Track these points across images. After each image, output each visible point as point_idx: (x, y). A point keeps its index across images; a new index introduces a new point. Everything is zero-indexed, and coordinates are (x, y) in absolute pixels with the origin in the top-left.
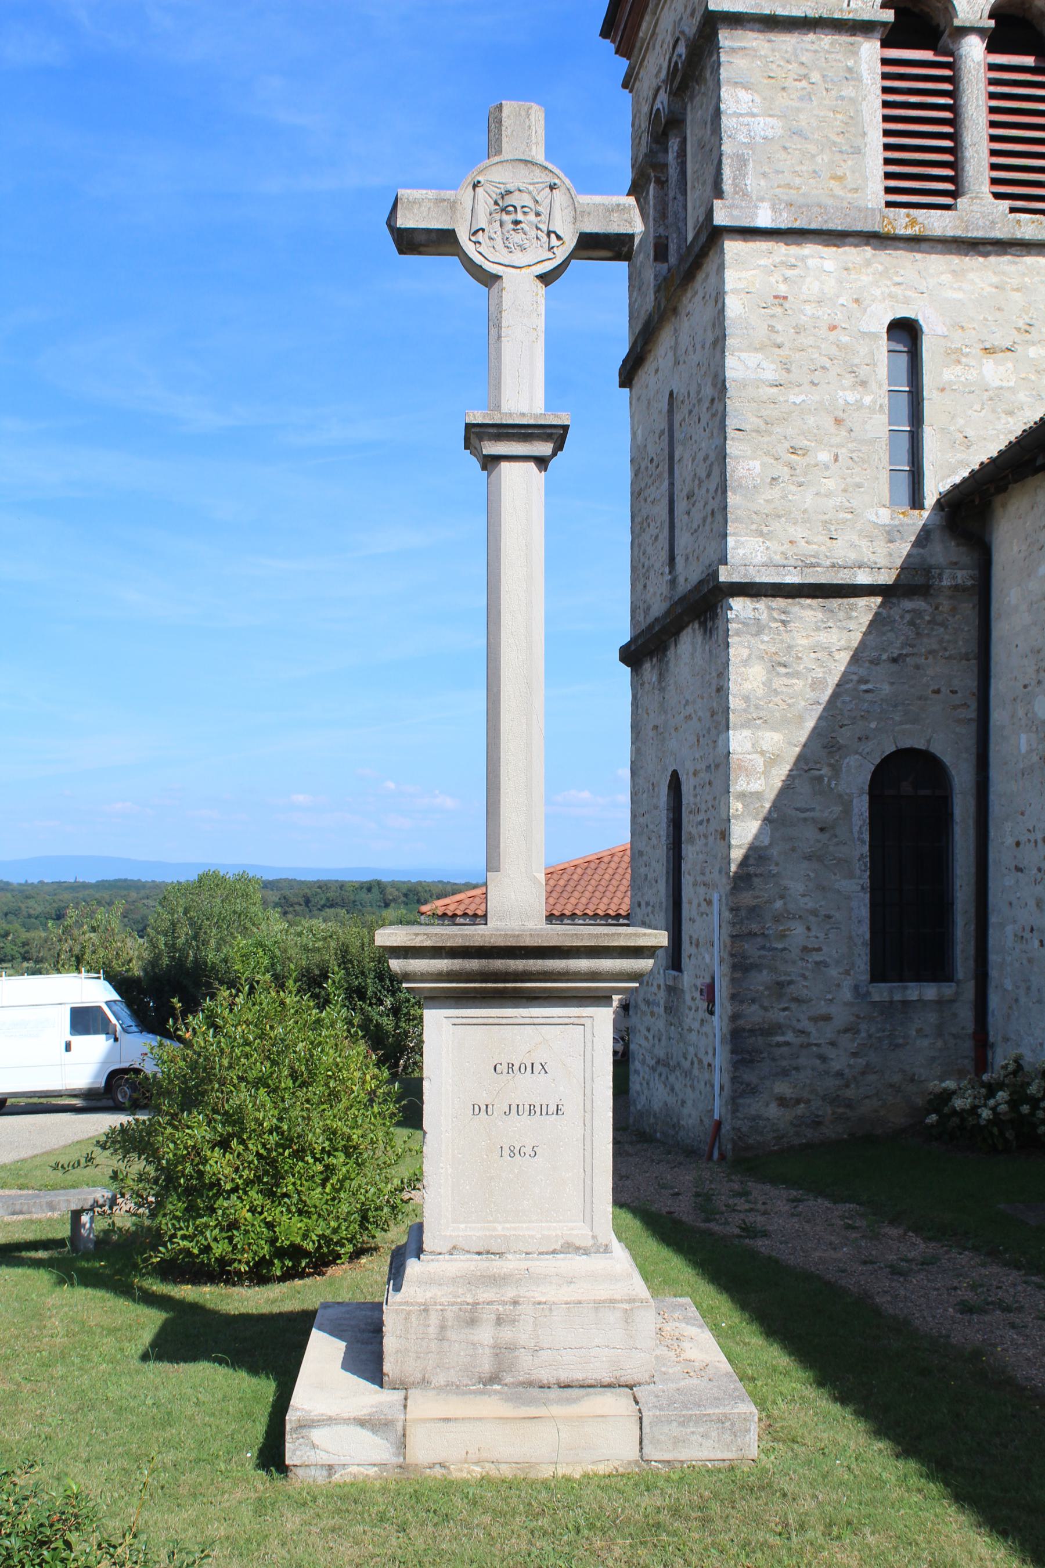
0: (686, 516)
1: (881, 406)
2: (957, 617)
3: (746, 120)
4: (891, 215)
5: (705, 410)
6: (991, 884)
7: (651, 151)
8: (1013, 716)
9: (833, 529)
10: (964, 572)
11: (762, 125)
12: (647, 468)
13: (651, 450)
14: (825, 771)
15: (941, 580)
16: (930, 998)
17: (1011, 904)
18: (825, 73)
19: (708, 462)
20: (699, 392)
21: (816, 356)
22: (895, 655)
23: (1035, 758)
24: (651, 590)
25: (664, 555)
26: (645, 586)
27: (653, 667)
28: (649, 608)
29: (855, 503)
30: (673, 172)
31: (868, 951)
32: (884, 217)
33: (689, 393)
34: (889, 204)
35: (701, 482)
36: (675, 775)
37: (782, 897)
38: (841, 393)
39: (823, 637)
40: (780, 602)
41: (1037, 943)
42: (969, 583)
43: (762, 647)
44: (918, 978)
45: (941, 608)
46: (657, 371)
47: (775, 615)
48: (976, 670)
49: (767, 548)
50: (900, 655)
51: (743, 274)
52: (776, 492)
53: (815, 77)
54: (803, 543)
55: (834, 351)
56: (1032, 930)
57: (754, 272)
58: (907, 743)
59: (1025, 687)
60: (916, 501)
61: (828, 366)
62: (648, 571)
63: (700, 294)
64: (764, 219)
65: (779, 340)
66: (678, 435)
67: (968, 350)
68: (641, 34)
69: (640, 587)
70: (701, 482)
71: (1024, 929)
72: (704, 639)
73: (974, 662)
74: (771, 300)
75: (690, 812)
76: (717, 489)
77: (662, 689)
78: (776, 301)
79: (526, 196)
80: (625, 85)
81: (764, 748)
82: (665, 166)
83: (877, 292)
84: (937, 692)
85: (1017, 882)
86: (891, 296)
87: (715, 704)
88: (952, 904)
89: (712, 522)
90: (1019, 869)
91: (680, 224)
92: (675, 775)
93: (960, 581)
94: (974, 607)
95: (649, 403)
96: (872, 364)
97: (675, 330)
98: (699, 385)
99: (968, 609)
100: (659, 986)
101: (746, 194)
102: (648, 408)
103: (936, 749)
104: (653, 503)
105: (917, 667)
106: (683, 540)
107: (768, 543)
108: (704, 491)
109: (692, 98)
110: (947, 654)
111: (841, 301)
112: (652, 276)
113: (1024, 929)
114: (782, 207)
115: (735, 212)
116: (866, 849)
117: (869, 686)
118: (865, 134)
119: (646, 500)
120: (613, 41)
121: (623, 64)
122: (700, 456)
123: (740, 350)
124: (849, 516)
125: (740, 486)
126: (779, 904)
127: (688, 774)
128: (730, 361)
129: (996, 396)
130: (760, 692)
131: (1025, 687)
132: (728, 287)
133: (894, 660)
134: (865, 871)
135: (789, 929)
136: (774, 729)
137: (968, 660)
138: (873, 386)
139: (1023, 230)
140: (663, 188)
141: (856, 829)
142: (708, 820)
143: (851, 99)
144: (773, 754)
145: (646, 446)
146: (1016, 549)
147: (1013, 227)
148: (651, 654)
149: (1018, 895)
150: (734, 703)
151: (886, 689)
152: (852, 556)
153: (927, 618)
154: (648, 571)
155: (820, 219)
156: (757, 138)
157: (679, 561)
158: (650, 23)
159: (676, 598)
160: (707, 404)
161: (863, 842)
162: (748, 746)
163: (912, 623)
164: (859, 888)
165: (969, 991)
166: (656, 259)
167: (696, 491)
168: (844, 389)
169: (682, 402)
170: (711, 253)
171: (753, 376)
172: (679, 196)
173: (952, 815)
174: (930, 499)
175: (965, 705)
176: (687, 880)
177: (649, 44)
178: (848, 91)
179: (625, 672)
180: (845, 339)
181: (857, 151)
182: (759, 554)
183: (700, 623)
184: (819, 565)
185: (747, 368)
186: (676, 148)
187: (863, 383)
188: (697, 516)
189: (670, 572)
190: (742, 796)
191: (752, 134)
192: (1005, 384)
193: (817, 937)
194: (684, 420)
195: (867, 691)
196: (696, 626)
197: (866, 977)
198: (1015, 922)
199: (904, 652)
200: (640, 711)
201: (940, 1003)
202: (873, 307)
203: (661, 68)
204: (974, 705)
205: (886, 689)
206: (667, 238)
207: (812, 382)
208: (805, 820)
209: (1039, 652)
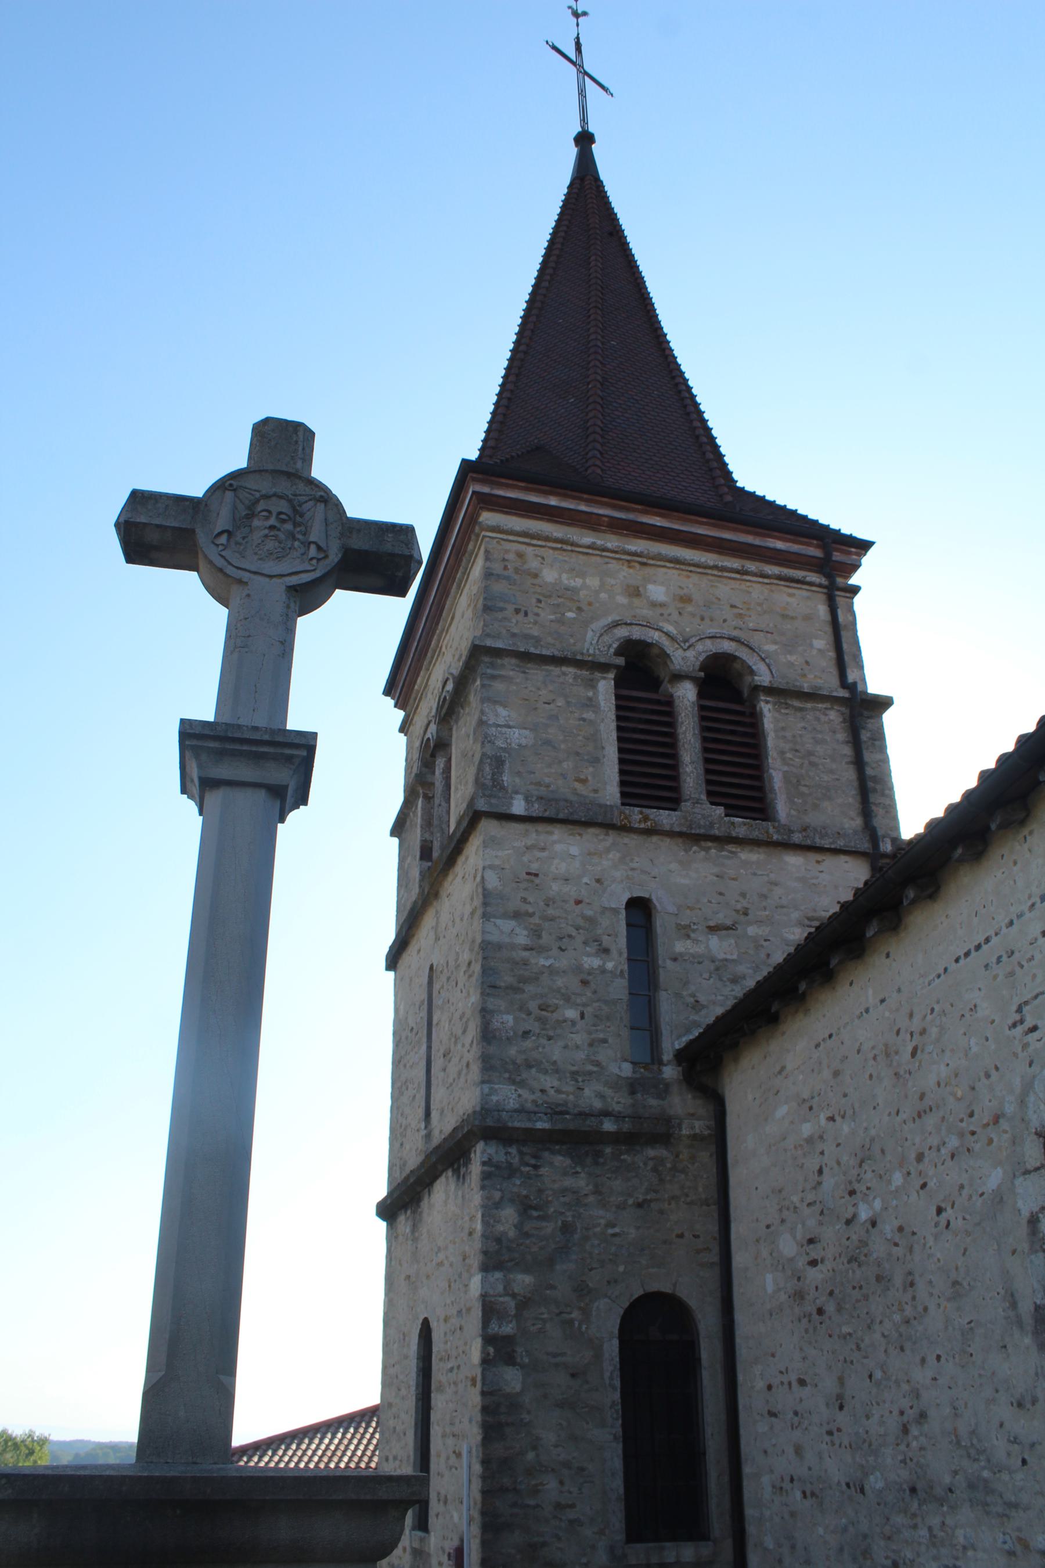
0: (442, 1074)
1: (622, 971)
2: (696, 1164)
3: (504, 730)
4: (627, 812)
5: (462, 973)
6: (742, 1431)
7: (421, 772)
8: (756, 1258)
9: (580, 1079)
10: (701, 1122)
11: (516, 735)
12: (407, 1038)
13: (411, 1022)
14: (575, 1315)
15: (680, 1130)
16: (688, 1560)
17: (765, 1452)
18: (570, 700)
19: (464, 1020)
20: (457, 960)
21: (563, 925)
22: (640, 1200)
23: (783, 1297)
24: (408, 1147)
25: (421, 1112)
26: (402, 1145)
27: (407, 1219)
28: (404, 1164)
29: (600, 1057)
30: (439, 785)
31: (623, 1508)
32: (621, 813)
33: (447, 962)
35: (457, 1039)
36: (426, 1323)
37: (534, 1448)
38: (585, 959)
41: (798, 1495)
42: (706, 1132)
43: (515, 1190)
44: (674, 1538)
45: (681, 1156)
46: (419, 951)
47: (527, 1158)
48: (716, 1215)
49: (520, 1096)
50: (645, 1200)
51: (500, 853)
52: (528, 1044)
54: (552, 1092)
55: (580, 922)
56: (792, 1480)
57: (509, 852)
58: (654, 1287)
59: (768, 1227)
61: (573, 934)
62: (405, 1129)
63: (460, 876)
65: (531, 910)
66: (437, 1001)
67: (695, 927)
68: (416, 687)
69: (398, 1145)
70: (457, 1039)
71: (782, 1479)
72: (457, 1185)
73: (714, 1207)
74: (524, 876)
75: (441, 1359)
76: (472, 1042)
77: (415, 1240)
78: (528, 877)
79: (283, 503)
80: (402, 729)
81: (516, 1291)
82: (433, 784)
84: (681, 1236)
85: (772, 1428)
86: (628, 877)
87: (467, 1248)
88: (704, 1454)
89: (467, 1074)
90: (772, 1414)
91: (444, 826)
92: (426, 1323)
93: (697, 1131)
94: (711, 1156)
95: (411, 980)
97: (437, 912)
98: (457, 954)
99: (706, 1157)
100: (405, 1549)
101: (503, 788)
102: (410, 985)
103: (683, 1293)
104: (411, 1067)
105: (661, 1212)
106: (439, 1094)
107: (520, 1091)
108: (459, 1046)
109: (457, 722)
110: (689, 1199)
111: (585, 880)
112: (418, 873)
113: (782, 1479)
114: (534, 800)
115: (493, 801)
116: (617, 1396)
117: (617, 1230)
118: (603, 748)
119: (405, 1066)
120: (393, 698)
121: (400, 714)
122: (457, 1015)
123: (495, 917)
124: (595, 1069)
125: (494, 1037)
126: (531, 1456)
127: (438, 1321)
129: (720, 967)
130: (512, 1234)
131: (768, 1227)
133: (639, 1205)
134: (617, 1419)
135: (542, 1484)
136: (527, 1271)
137: (708, 1205)
138: (614, 953)
139: (737, 830)
140: (429, 802)
141: (607, 1375)
142: (459, 1367)
143: (591, 721)
144: (525, 1297)
145: (407, 1018)
146: (750, 1097)
147: (729, 827)
148: (404, 1207)
149: (774, 1441)
151: (633, 1233)
152: (598, 1104)
153: (669, 1165)
154: (405, 1129)
155: (566, 811)
156: (513, 745)
157: (435, 1115)
158: (424, 677)
159: (431, 1149)
160: (464, 968)
161: (614, 1388)
162: (500, 1288)
163: (655, 1170)
164: (612, 1437)
165: (727, 1547)
166: (422, 858)
167: (452, 1049)
168: (589, 955)
169: (441, 972)
170: (470, 839)
171: (507, 940)
172: (443, 804)
173: (699, 1359)
175: (708, 1249)
176: (435, 1431)
177: (422, 694)
178: (589, 715)
179: (383, 1225)
181: (596, 761)
182: (511, 1101)
183: (454, 1171)
184: (567, 1113)
185: (502, 932)
186: (442, 766)
187: (606, 951)
188: (453, 1069)
189: (426, 1127)
191: (509, 741)
192: (729, 957)
193: (570, 1493)
194: (442, 987)
195: (614, 1235)
196: (450, 1173)
197: (621, 1537)
198: (772, 1472)
199: (648, 1197)
200: (393, 1263)
202: (613, 886)
203: (431, 709)
204: (716, 1249)
205: (633, 1233)
206: (432, 842)
207: (560, 948)
208: (557, 1365)
209: (780, 1191)
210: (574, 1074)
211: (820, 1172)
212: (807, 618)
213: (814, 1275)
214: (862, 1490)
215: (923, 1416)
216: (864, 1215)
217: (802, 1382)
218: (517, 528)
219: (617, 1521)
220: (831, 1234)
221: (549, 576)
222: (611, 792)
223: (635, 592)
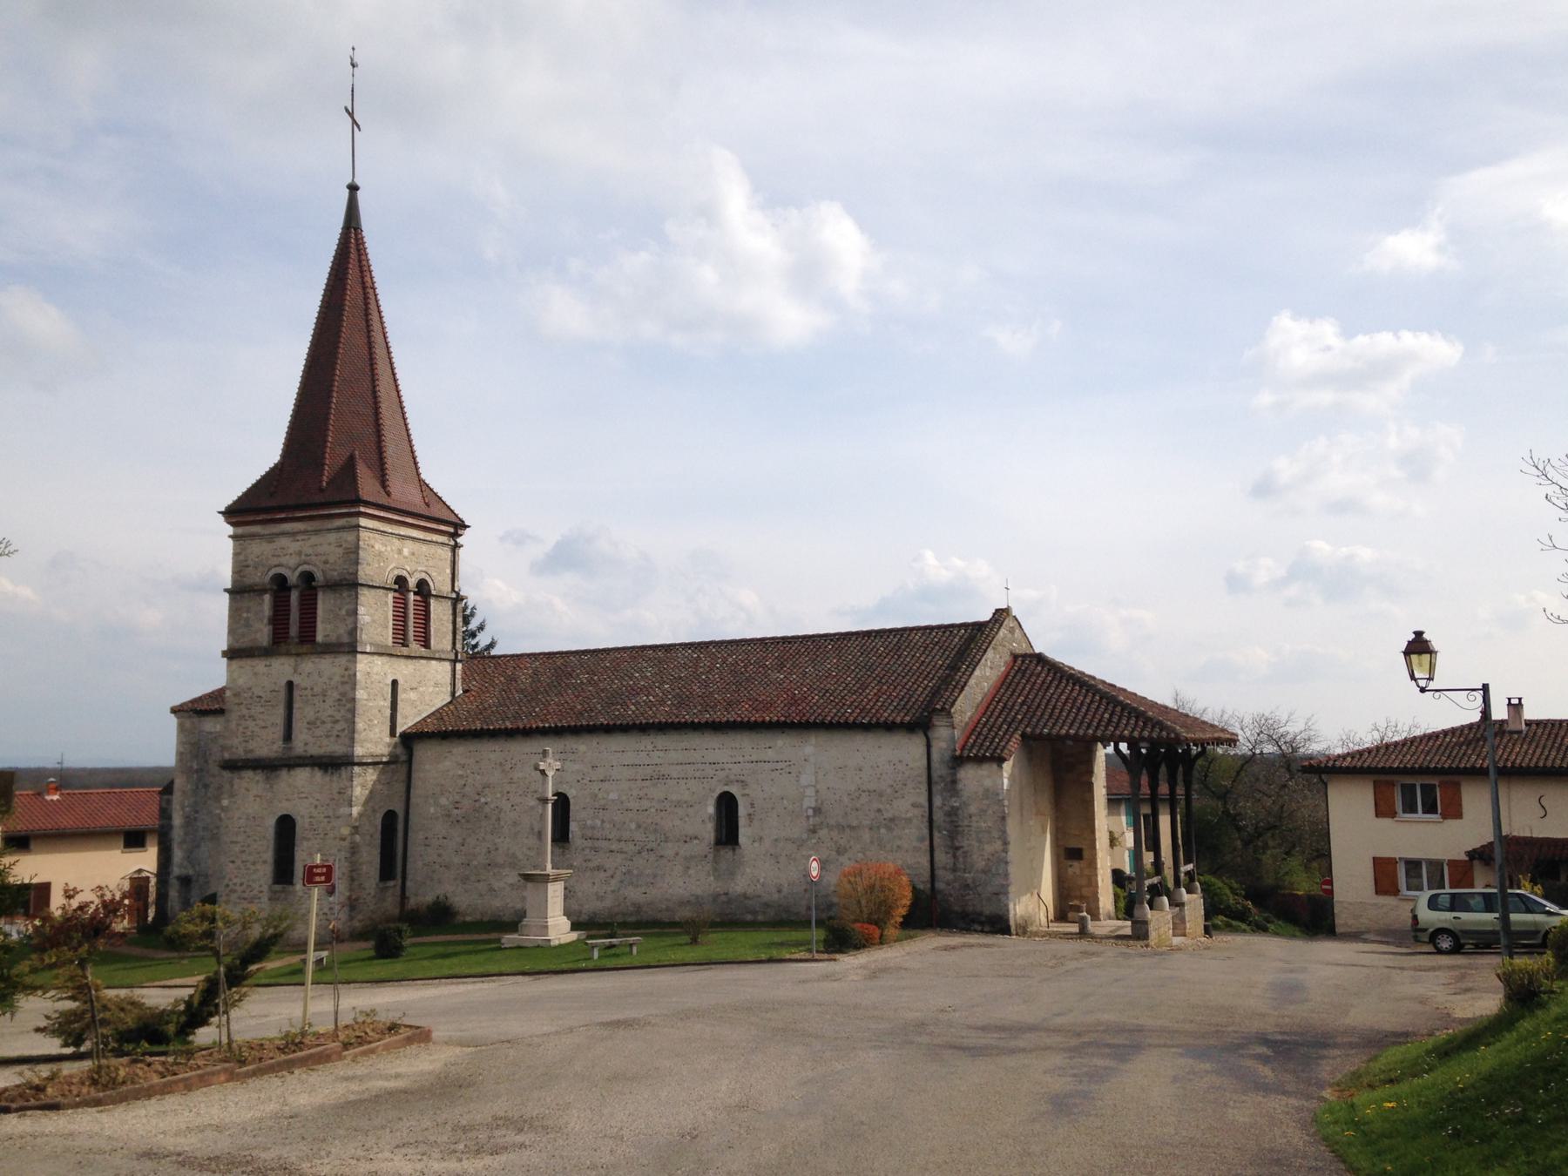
34: (394, 643)
40: (365, 767)
60: (393, 733)
64: (368, 651)
103: (397, 810)
151: (386, 792)
174: (398, 735)
181: (387, 627)
201: (395, 886)
205: (386, 792)
213: (456, 811)
215: (497, 849)
216: (483, 800)
217: (444, 838)
218: (371, 526)
220: (466, 803)
222: (390, 641)
223: (400, 552)
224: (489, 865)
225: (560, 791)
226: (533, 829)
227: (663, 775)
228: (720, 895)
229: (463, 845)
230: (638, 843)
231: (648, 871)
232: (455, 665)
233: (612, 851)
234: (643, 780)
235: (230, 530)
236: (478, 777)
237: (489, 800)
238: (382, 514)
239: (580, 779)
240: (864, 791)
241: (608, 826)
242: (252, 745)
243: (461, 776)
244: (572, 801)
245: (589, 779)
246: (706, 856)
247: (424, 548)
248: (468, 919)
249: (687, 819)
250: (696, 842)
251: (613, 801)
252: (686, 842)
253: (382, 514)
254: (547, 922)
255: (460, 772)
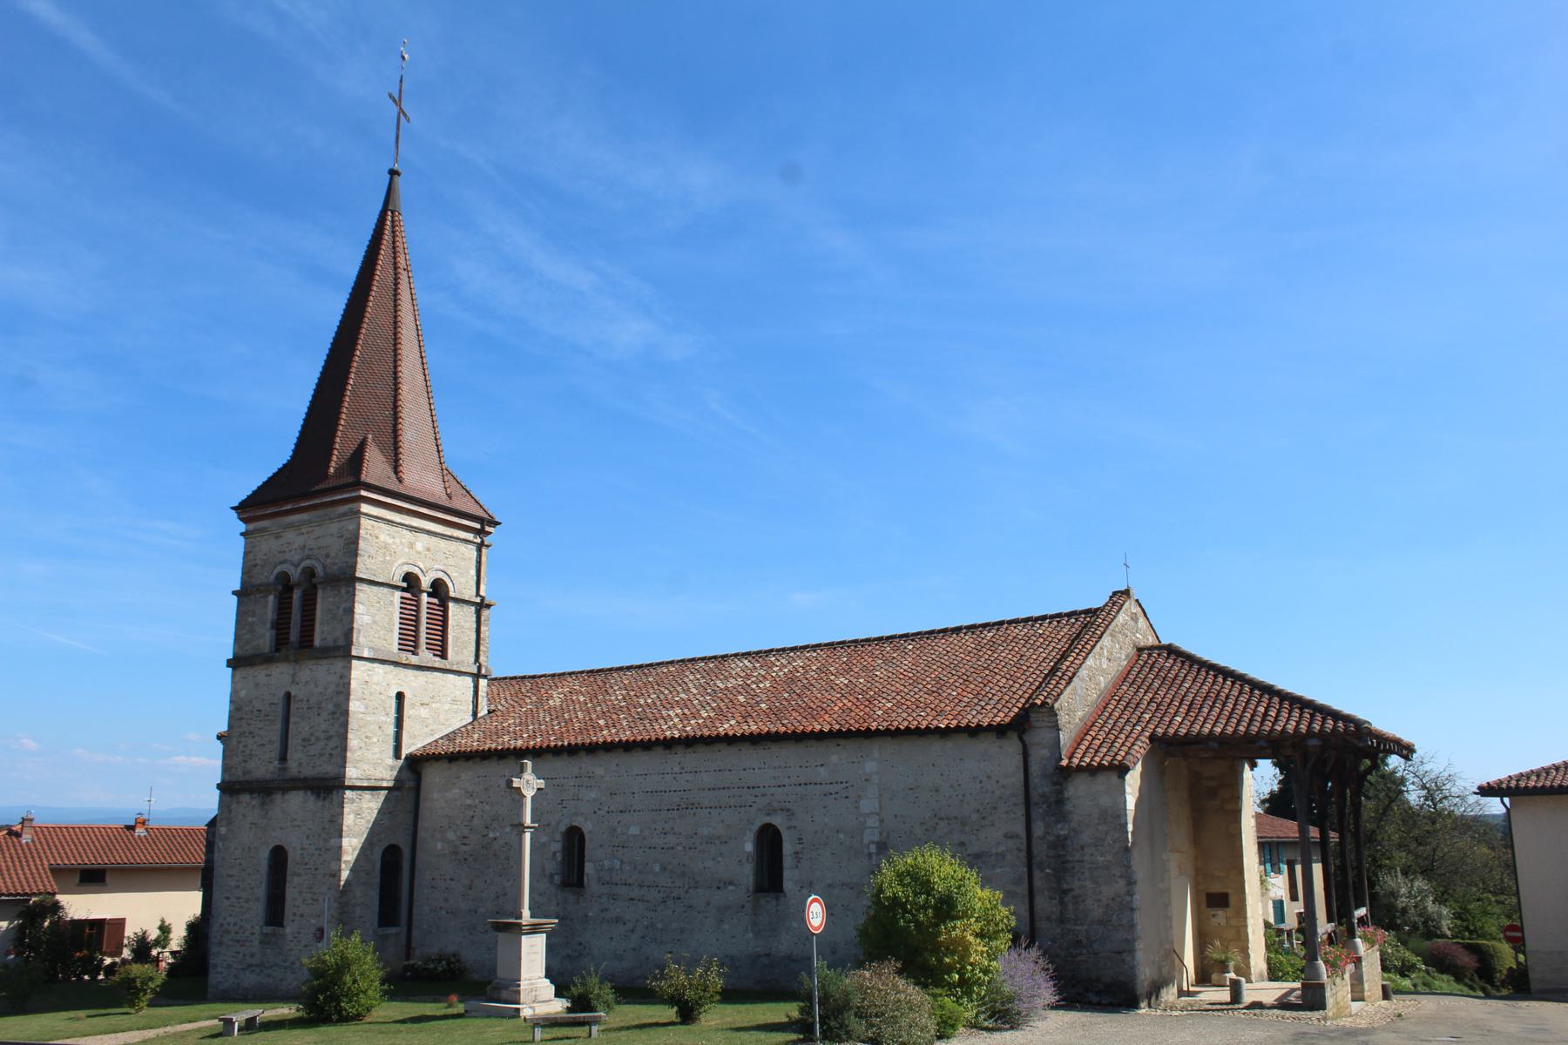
34: (400, 649)
39: (371, 805)
40: (359, 792)
53: (382, 603)
60: (397, 754)
64: (366, 655)
83: (394, 682)
86: (398, 684)
96: (391, 707)
103: (400, 845)
126: (353, 901)
128: (351, 704)
132: (352, 677)
136: (355, 838)
150: (345, 828)
165: (405, 929)
174: (403, 757)
180: (383, 698)
181: (392, 631)
187: (388, 714)
190: (345, 862)
210: (374, 764)
211: (473, 817)
212: (470, 559)
213: (464, 848)
214: (476, 912)
215: (505, 894)
216: (491, 835)
217: (451, 879)
218: (375, 514)
219: (376, 922)
221: (382, 537)
222: (395, 647)
223: (411, 545)
224: (497, 913)
225: (574, 824)
226: (544, 871)
227: (693, 804)
228: (760, 956)
229: (470, 889)
230: (662, 889)
231: (674, 925)
232: (478, 681)
233: (632, 899)
234: (668, 810)
235: (242, 527)
236: (487, 807)
237: (498, 834)
238: (389, 500)
239: (596, 810)
240: (942, 819)
241: (628, 868)
242: (251, 765)
243: (469, 806)
244: (587, 836)
245: (606, 809)
246: (743, 907)
247: (443, 543)
248: (475, 976)
249: (720, 859)
250: (731, 888)
251: (635, 836)
252: (719, 888)
253: (389, 500)
254: (519, 986)
255: (469, 802)
